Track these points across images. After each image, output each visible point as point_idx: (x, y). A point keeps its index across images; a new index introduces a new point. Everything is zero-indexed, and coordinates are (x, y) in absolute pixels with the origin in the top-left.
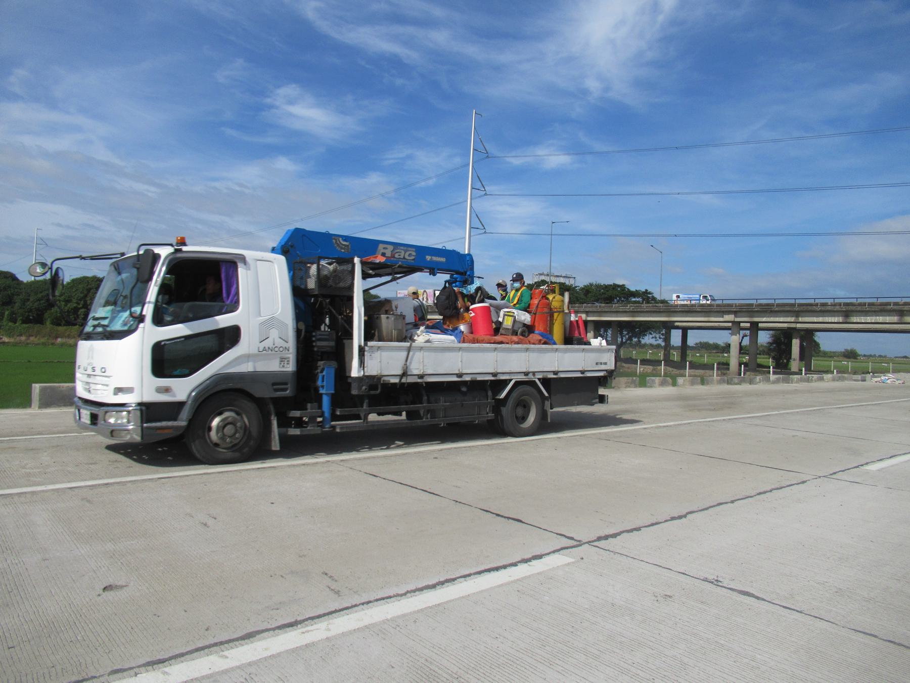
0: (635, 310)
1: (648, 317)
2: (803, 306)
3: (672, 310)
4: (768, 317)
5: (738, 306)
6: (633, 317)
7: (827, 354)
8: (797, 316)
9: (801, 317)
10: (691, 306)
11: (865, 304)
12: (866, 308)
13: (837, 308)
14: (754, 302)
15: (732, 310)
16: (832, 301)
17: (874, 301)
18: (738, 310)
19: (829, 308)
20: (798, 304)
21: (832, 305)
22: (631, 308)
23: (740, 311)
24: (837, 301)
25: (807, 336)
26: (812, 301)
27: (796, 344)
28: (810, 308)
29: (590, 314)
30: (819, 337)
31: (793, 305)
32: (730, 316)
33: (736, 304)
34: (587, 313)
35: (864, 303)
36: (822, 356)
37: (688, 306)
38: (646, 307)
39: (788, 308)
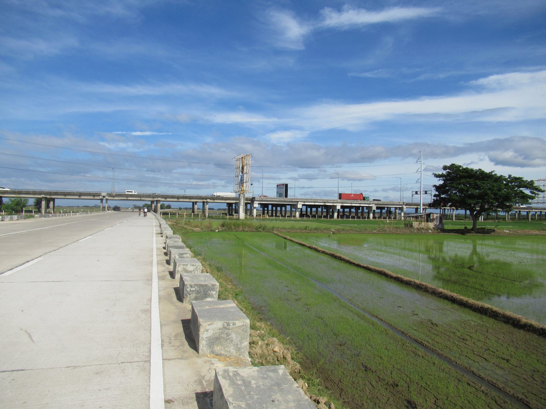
11: (85, 193)
13: (77, 194)
14: (52, 191)
17: (87, 192)
19: (75, 194)
21: (76, 193)
25: (53, 200)
26: (70, 192)
27: (43, 203)
28: (70, 194)
31: (65, 193)
39: (62, 193)
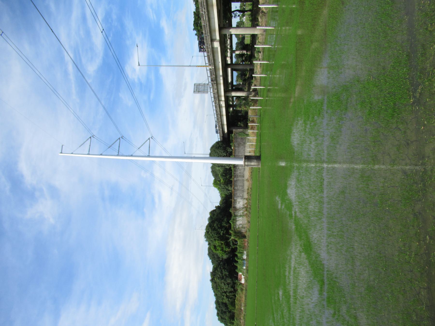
0: (205, 7)
6: (212, 5)
22: (203, 10)
29: (214, 38)
34: (212, 40)
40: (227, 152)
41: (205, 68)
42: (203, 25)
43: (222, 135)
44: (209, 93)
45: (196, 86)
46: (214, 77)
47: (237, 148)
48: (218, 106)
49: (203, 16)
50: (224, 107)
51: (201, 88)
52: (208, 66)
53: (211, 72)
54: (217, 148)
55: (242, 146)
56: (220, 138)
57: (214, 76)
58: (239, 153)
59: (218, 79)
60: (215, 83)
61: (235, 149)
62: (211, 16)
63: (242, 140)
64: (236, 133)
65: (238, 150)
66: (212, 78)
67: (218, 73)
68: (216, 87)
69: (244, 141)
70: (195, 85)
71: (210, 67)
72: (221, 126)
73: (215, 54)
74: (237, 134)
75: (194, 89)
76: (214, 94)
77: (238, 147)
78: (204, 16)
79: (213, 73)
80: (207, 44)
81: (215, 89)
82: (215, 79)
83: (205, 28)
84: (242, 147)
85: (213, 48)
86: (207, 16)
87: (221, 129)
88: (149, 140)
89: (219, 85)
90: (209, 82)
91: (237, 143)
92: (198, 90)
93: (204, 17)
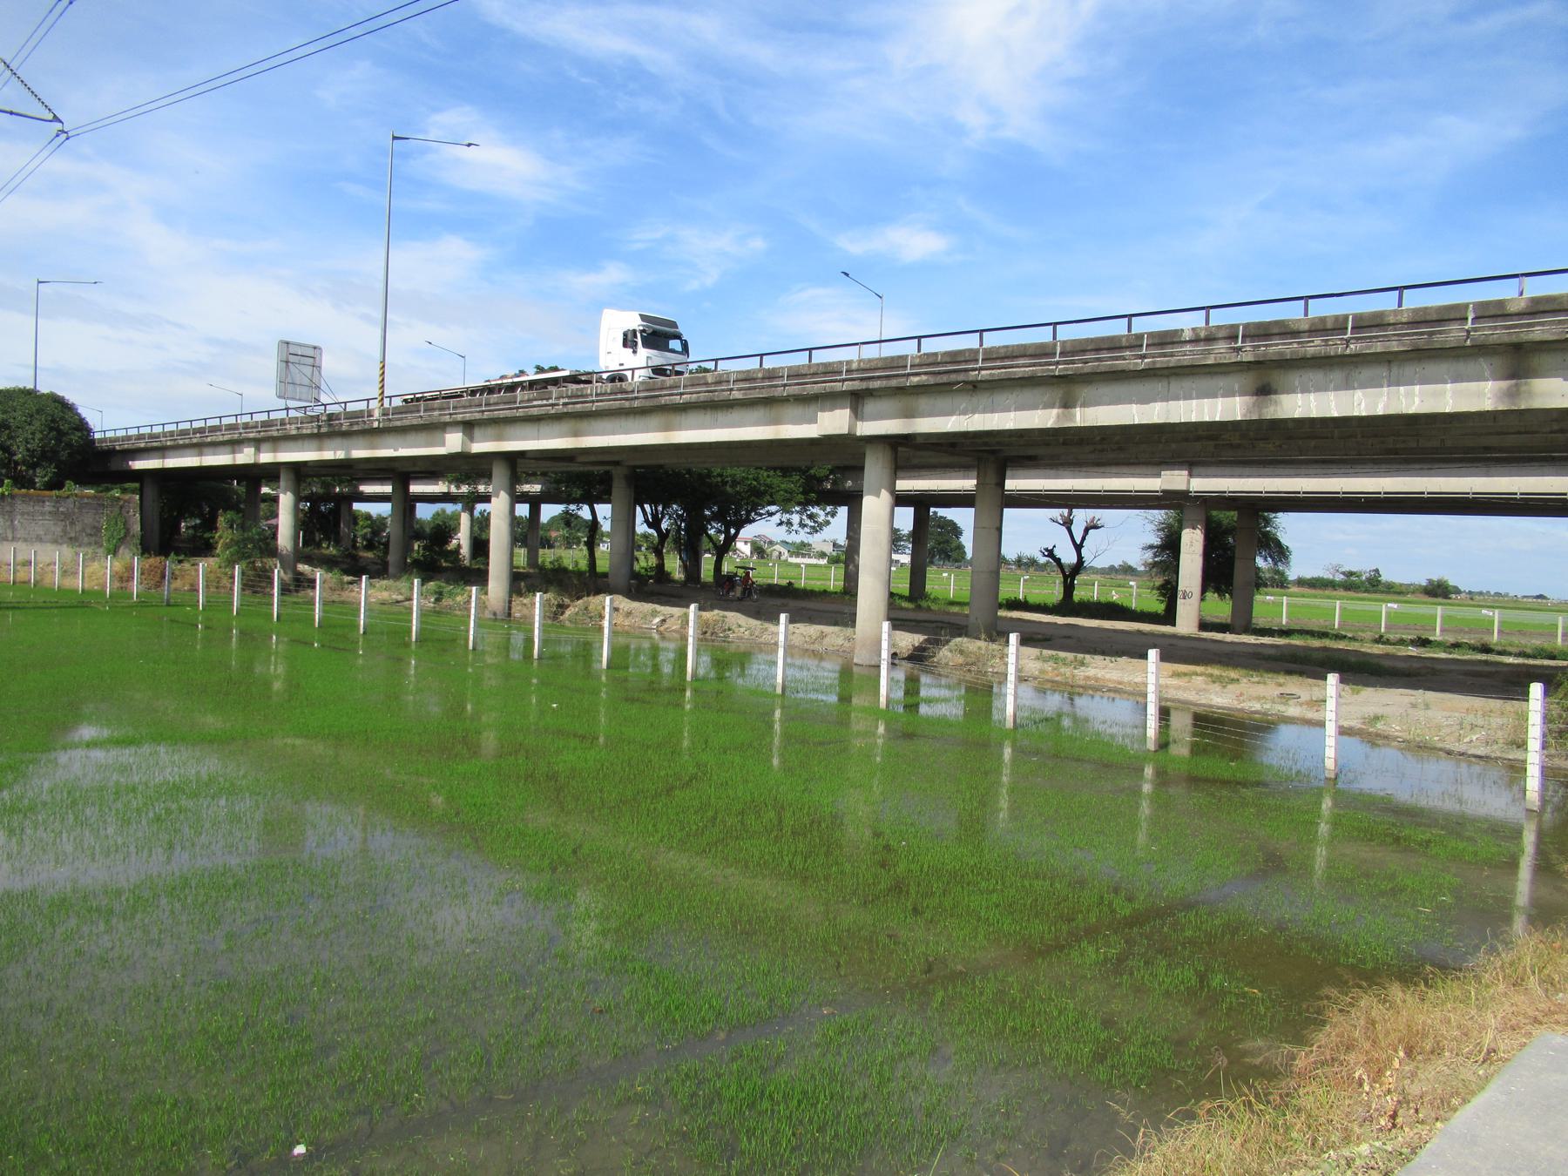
0: (570, 408)
1: (613, 433)
2: (1084, 351)
3: (663, 401)
4: (964, 413)
5: (858, 370)
6: (576, 434)
7: (1392, 587)
8: (1067, 404)
9: (1084, 405)
10: (719, 383)
12: (1348, 341)
13: (1220, 352)
14: (909, 348)
15: (838, 386)
16: (1194, 321)
18: (857, 385)
19: (1186, 355)
20: (1064, 343)
21: (1195, 341)
22: (562, 401)
23: (870, 393)
24: (1219, 319)
26: (1118, 329)
28: (1109, 363)
29: (477, 432)
30: (1288, 526)
31: (1041, 352)
32: (838, 412)
33: (849, 363)
34: (468, 427)
35: (1337, 318)
36: (1382, 592)
37: (706, 384)
38: (597, 395)
39: (1022, 369)
40: (34, 466)
41: (376, 393)
42: (516, 397)
43: (118, 448)
44: (281, 403)
45: (310, 352)
46: (341, 424)
47: (48, 507)
48: (236, 436)
49: (542, 400)
50: (234, 459)
51: (301, 373)
52: (382, 405)
53: (359, 414)
54: (53, 421)
55: (59, 529)
56: (102, 441)
57: (344, 428)
58: (26, 516)
59: (338, 441)
60: (319, 427)
61: (44, 502)
62: (545, 428)
63: (89, 531)
64: (121, 507)
65: (43, 514)
66: (340, 419)
67: (360, 441)
68: (309, 432)
69: (86, 540)
70: (315, 348)
71: (377, 414)
72: (155, 444)
73: (422, 437)
74: (117, 509)
75: (300, 345)
76: (283, 422)
77: (55, 514)
78: (545, 402)
79: (357, 423)
80: (454, 408)
81: (298, 428)
82: (337, 428)
83: (505, 403)
84: (58, 530)
85: (440, 427)
86: (543, 411)
87: (142, 445)
88: (50, 117)
89: (314, 443)
90: (325, 405)
91: (76, 510)
92: (292, 358)
93: (540, 402)
